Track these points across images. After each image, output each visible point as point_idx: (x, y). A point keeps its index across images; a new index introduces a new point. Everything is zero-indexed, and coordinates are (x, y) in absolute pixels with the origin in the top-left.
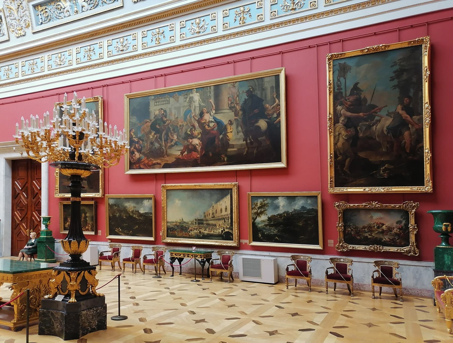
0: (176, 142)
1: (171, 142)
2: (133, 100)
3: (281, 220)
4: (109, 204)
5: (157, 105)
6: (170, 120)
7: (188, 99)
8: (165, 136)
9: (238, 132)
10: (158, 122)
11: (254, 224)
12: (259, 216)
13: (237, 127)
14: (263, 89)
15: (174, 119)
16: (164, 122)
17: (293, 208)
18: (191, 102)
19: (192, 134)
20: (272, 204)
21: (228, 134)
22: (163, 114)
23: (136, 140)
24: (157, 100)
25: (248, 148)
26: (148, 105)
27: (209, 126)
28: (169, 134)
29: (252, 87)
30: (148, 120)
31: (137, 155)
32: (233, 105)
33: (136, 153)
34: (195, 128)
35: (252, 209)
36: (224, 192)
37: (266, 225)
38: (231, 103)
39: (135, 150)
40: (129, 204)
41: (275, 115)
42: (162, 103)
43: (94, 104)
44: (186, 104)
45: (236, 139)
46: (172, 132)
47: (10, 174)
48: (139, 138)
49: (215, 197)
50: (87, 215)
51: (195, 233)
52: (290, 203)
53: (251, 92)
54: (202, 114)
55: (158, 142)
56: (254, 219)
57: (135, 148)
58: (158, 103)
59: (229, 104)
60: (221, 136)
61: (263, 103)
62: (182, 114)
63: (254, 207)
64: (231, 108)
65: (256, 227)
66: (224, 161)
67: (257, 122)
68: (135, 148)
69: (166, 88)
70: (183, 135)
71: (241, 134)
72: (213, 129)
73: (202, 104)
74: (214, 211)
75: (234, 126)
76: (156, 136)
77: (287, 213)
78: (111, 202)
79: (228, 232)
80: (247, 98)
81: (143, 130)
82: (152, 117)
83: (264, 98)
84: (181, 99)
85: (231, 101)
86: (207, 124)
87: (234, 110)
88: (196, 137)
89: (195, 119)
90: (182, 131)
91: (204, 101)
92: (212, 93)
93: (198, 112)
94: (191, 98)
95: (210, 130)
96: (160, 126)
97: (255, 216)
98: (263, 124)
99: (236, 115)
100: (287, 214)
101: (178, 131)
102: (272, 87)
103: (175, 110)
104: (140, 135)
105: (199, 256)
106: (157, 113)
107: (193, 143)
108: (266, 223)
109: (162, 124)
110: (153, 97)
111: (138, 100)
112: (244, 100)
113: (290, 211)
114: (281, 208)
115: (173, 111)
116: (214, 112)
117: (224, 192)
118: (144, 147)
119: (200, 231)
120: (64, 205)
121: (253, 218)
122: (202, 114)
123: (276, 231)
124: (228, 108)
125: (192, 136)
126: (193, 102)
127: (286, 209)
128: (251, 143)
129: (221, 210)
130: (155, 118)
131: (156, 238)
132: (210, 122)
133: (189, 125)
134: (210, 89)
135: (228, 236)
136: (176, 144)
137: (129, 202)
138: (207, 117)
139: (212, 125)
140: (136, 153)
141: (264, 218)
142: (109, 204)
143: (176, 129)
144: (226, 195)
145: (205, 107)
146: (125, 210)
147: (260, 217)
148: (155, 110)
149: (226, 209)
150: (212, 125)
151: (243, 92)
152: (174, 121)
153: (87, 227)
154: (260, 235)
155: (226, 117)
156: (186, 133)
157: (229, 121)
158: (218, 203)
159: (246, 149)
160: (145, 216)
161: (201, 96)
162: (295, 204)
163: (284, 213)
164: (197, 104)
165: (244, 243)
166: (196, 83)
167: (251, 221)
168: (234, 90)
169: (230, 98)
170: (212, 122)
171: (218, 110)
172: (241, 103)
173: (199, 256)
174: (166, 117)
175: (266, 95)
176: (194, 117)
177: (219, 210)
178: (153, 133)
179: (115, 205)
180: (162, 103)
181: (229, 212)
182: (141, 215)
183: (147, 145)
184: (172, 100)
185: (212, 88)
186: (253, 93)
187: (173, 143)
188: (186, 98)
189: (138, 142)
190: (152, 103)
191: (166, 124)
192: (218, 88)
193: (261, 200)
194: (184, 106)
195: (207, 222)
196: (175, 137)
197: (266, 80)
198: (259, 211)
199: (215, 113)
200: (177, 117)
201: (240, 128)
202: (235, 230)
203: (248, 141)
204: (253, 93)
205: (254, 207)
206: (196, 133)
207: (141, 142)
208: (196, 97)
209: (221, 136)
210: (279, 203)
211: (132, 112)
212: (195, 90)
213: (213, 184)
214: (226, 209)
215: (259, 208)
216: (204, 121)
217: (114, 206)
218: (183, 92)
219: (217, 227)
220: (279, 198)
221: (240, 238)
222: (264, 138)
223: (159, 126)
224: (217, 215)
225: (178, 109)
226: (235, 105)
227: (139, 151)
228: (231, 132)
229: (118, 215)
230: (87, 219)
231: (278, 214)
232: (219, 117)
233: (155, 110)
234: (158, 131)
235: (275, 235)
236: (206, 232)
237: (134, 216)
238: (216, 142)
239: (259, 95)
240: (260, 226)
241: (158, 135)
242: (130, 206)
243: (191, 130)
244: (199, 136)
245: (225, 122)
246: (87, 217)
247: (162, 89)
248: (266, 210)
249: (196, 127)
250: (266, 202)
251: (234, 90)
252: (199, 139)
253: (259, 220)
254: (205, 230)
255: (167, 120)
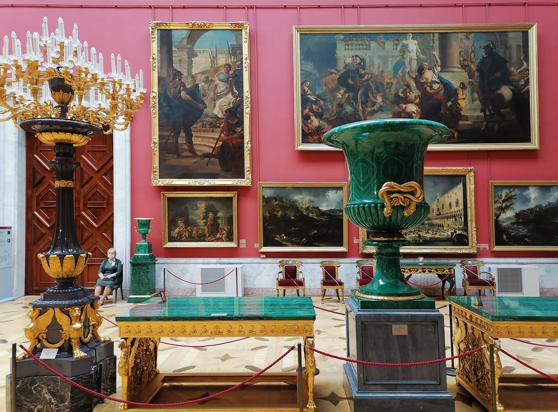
0: (381, 106)
1: (373, 106)
2: (307, 36)
3: (532, 216)
4: (263, 197)
5: (348, 50)
6: (372, 74)
7: (399, 47)
8: (363, 97)
9: (473, 100)
10: (351, 75)
11: (497, 222)
12: (504, 211)
13: (472, 93)
14: (507, 48)
15: (377, 73)
16: (362, 76)
17: (548, 200)
18: (404, 52)
19: (406, 97)
20: (521, 196)
21: (459, 101)
22: (360, 64)
23: (312, 98)
24: (349, 42)
25: (488, 122)
26: (332, 48)
27: (431, 87)
28: (370, 94)
29: (493, 43)
30: (333, 71)
31: (315, 122)
32: (466, 63)
33: (313, 118)
34: (411, 90)
35: (495, 202)
36: (459, 179)
37: (513, 224)
38: (464, 60)
39: (311, 114)
40: (300, 197)
41: (522, 82)
42: (358, 47)
43: (233, 34)
44: (396, 53)
45: (471, 109)
46: (375, 91)
47: (24, 142)
48: (319, 97)
49: (441, 186)
50: (220, 214)
51: (412, 237)
52: (543, 195)
53: (492, 49)
54: (421, 70)
55: (352, 105)
56: (497, 216)
57: (311, 110)
58: (350, 47)
59: (460, 61)
60: (449, 104)
61: (508, 65)
62: (390, 67)
63: (498, 201)
64: (463, 67)
65: (500, 225)
66: (454, 138)
67: (499, 88)
68: (311, 110)
69: (362, 26)
70: (392, 97)
71: (477, 102)
72: (437, 93)
73: (422, 56)
74: (440, 206)
75: (468, 91)
76: (347, 95)
77: (539, 207)
78: (268, 193)
79: (461, 234)
80: (485, 56)
81: (326, 85)
82: (341, 66)
83: (508, 59)
84: (389, 45)
85: (463, 57)
86: (429, 84)
87: (467, 69)
88: (412, 102)
89: (410, 76)
90: (390, 91)
91: (423, 52)
92: (437, 43)
93: (415, 66)
94: (405, 46)
95: (432, 95)
96: (354, 81)
97: (498, 212)
98: (506, 92)
99: (471, 76)
100: (540, 209)
101: (384, 91)
102: (518, 47)
103: (379, 60)
104: (319, 91)
105: (420, 270)
106: (349, 60)
107: (408, 110)
108: (513, 221)
109: (358, 78)
110: (342, 37)
111: (316, 38)
112: (481, 58)
113: (544, 205)
114: (532, 201)
115: (377, 62)
116: (439, 69)
117: (459, 179)
118: (328, 110)
119: (419, 235)
120: (169, 199)
121: (496, 215)
122: (421, 70)
123: (526, 230)
124: (460, 66)
125: (407, 101)
126: (407, 52)
127: (538, 203)
128: (491, 115)
129: (450, 205)
130: (345, 67)
131: (349, 248)
132: (432, 82)
133: (402, 83)
134: (434, 36)
135: (461, 240)
136: (380, 109)
137: (301, 194)
138: (429, 75)
139: (436, 86)
140: (313, 118)
141: (510, 214)
142: (263, 197)
143: (380, 88)
144: (457, 184)
145: (426, 61)
146: (293, 206)
147: (505, 213)
148: (345, 56)
149: (457, 203)
150: (436, 86)
151: (480, 47)
152: (377, 76)
153: (218, 236)
154: (505, 237)
155: (456, 77)
156: (396, 95)
157: (461, 83)
158: (446, 196)
159: (485, 123)
160: (329, 215)
161: (419, 44)
162: (550, 196)
163: (536, 207)
164: (413, 55)
165: (481, 249)
166: (414, 25)
167: (494, 218)
168: (468, 43)
169: (463, 54)
170: (436, 82)
171: (445, 67)
172: (478, 61)
173: (420, 270)
174: (364, 69)
175: (510, 54)
176: (408, 73)
177: (447, 205)
178: (342, 91)
179: (275, 199)
180: (358, 47)
181: (461, 207)
182: (323, 213)
183: (332, 108)
184: (373, 44)
185: (437, 36)
186: (494, 51)
187: (375, 108)
188: (397, 45)
189: (316, 102)
190: (340, 46)
191: (364, 79)
192: (444, 37)
193: (507, 191)
194: (393, 56)
195: (430, 222)
196: (380, 100)
197: (511, 35)
198: (504, 205)
199: (441, 71)
200: (383, 71)
201: (476, 95)
202: (472, 232)
203: (488, 113)
204: (494, 51)
205: (498, 201)
206: (412, 95)
207: (322, 102)
208: (413, 45)
209: (449, 104)
210: (530, 194)
211: (306, 56)
212: (411, 34)
213: (441, 168)
214: (457, 203)
215: (504, 201)
216: (425, 80)
217: (274, 201)
218: (393, 35)
219: (445, 228)
220: (530, 188)
221: (479, 241)
222: (508, 110)
223: (353, 81)
224: (443, 212)
225: (384, 59)
226: (470, 63)
227: (319, 116)
228: (464, 99)
229: (279, 214)
230: (220, 221)
231: (529, 209)
232: (446, 77)
233: (345, 56)
234: (350, 89)
235: (525, 236)
236: (429, 236)
237: (311, 215)
238: (442, 111)
239: (502, 55)
240: (505, 224)
241: (351, 94)
242: (303, 200)
243: (404, 92)
244: (417, 101)
245: (456, 84)
246: (219, 218)
247: (352, 26)
248: (513, 204)
249: (412, 87)
250: (513, 193)
251: (468, 43)
252: (416, 104)
253: (503, 216)
254: (426, 233)
255: (365, 74)
